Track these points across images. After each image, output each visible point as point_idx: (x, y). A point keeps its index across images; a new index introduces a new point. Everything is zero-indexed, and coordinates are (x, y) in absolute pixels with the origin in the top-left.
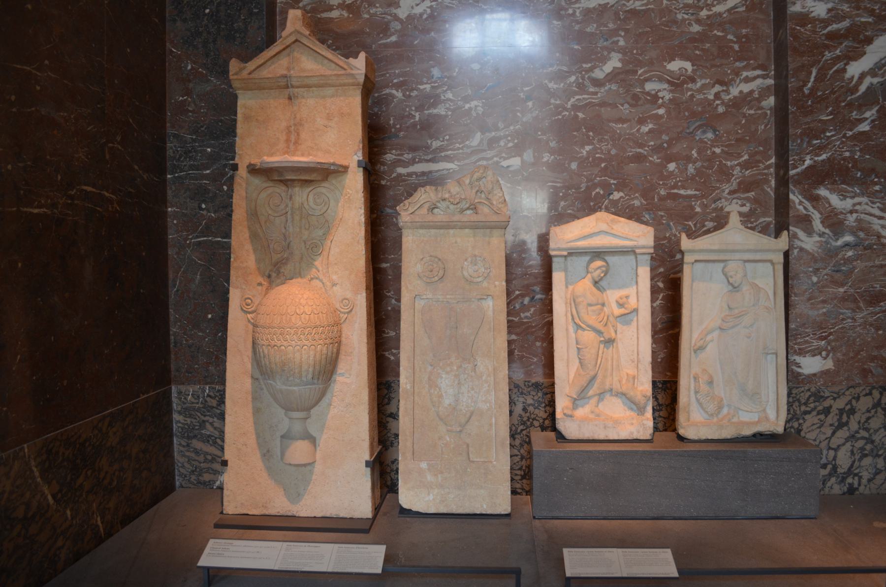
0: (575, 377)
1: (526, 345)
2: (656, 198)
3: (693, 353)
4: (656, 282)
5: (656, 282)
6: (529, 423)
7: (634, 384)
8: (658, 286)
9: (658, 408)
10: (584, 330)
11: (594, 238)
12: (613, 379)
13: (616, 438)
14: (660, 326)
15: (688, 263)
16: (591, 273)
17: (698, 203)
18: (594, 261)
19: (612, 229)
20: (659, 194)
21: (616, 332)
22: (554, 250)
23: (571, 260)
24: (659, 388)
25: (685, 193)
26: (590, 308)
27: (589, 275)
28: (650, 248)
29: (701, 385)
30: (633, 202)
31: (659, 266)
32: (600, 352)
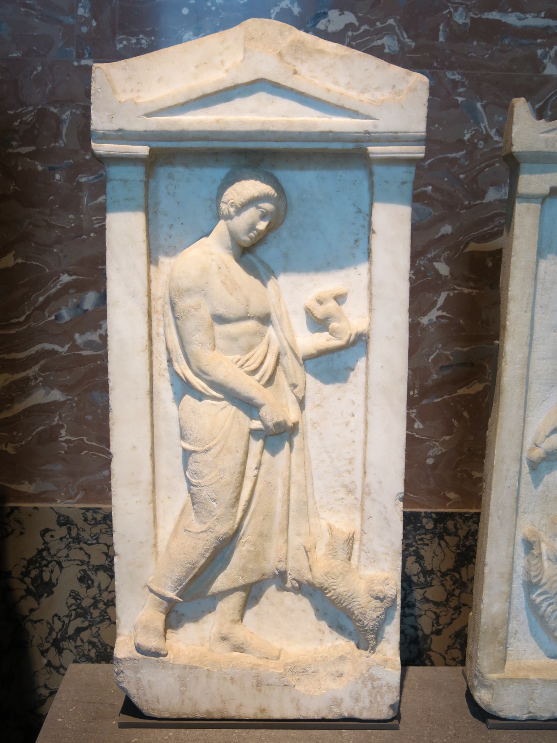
0: (175, 534)
1: (90, 418)
2: (441, 33)
3: (526, 469)
4: (431, 260)
5: (431, 260)
6: (96, 613)
7: (349, 559)
8: (437, 272)
9: (422, 579)
10: (200, 396)
11: (238, 103)
12: (287, 541)
13: (290, 713)
14: (435, 376)
15: (529, 198)
16: (229, 217)
17: (552, 53)
18: (238, 180)
19: (295, 73)
20: (449, 21)
21: (302, 403)
22: (105, 137)
23: (170, 176)
24: (427, 532)
25: (519, 24)
26: (220, 329)
27: (222, 225)
28: (415, 141)
29: (546, 564)
30: (379, 42)
31: (441, 220)
32: (252, 463)
